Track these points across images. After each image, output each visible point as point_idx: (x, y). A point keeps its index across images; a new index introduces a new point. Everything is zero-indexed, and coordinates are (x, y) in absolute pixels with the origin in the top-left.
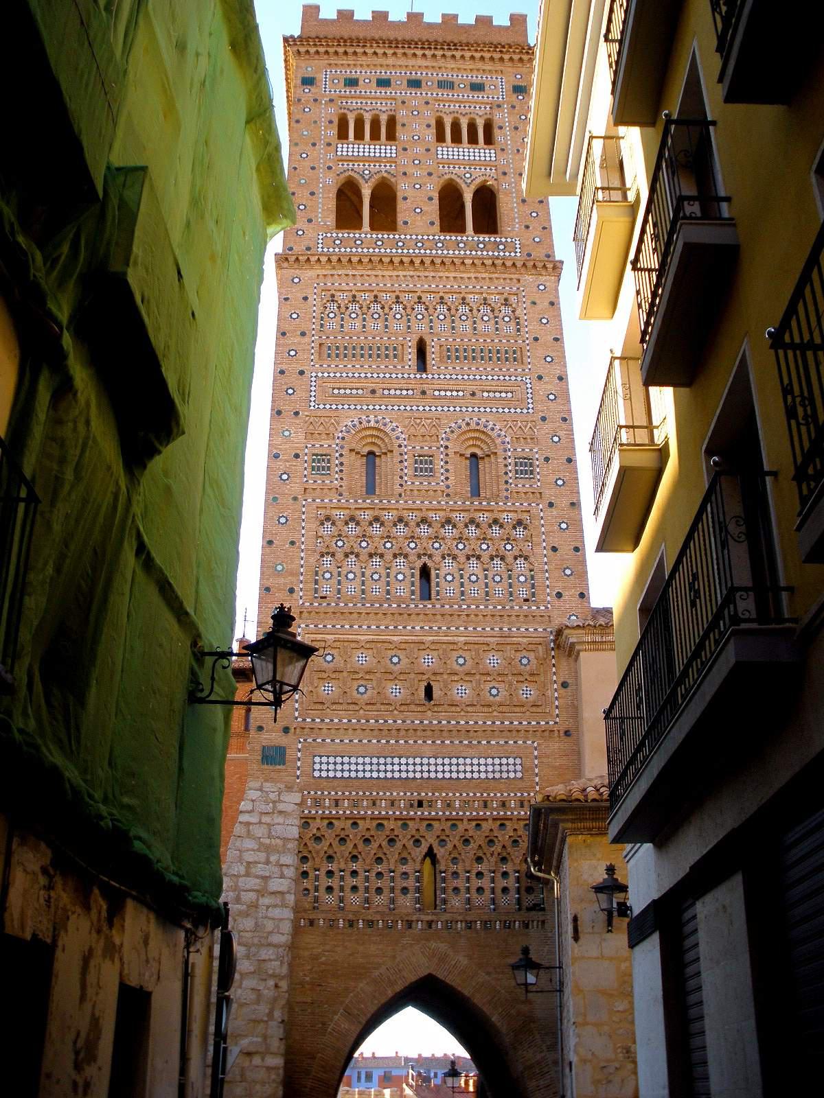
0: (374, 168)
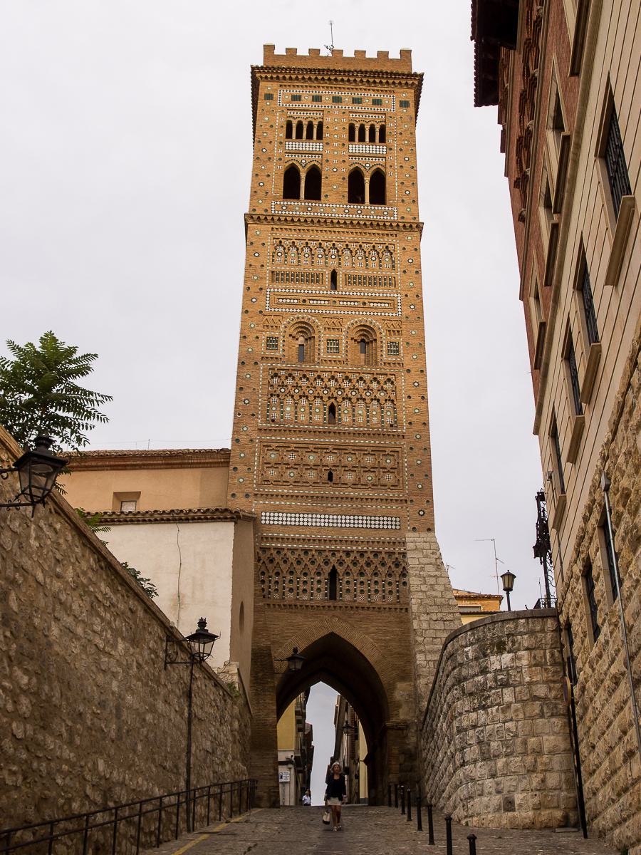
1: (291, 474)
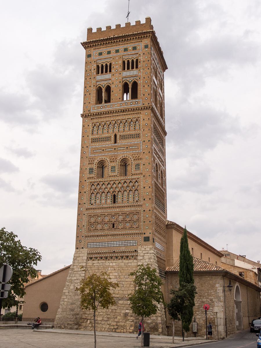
0: (105, 82)
1: (99, 227)
